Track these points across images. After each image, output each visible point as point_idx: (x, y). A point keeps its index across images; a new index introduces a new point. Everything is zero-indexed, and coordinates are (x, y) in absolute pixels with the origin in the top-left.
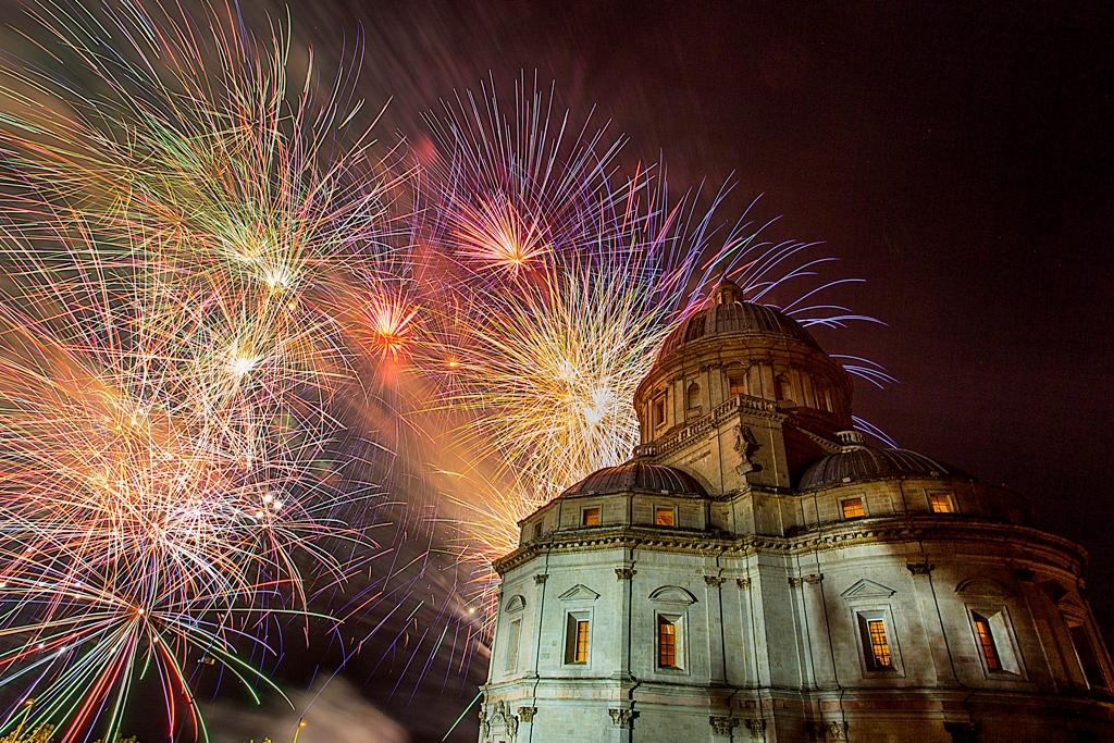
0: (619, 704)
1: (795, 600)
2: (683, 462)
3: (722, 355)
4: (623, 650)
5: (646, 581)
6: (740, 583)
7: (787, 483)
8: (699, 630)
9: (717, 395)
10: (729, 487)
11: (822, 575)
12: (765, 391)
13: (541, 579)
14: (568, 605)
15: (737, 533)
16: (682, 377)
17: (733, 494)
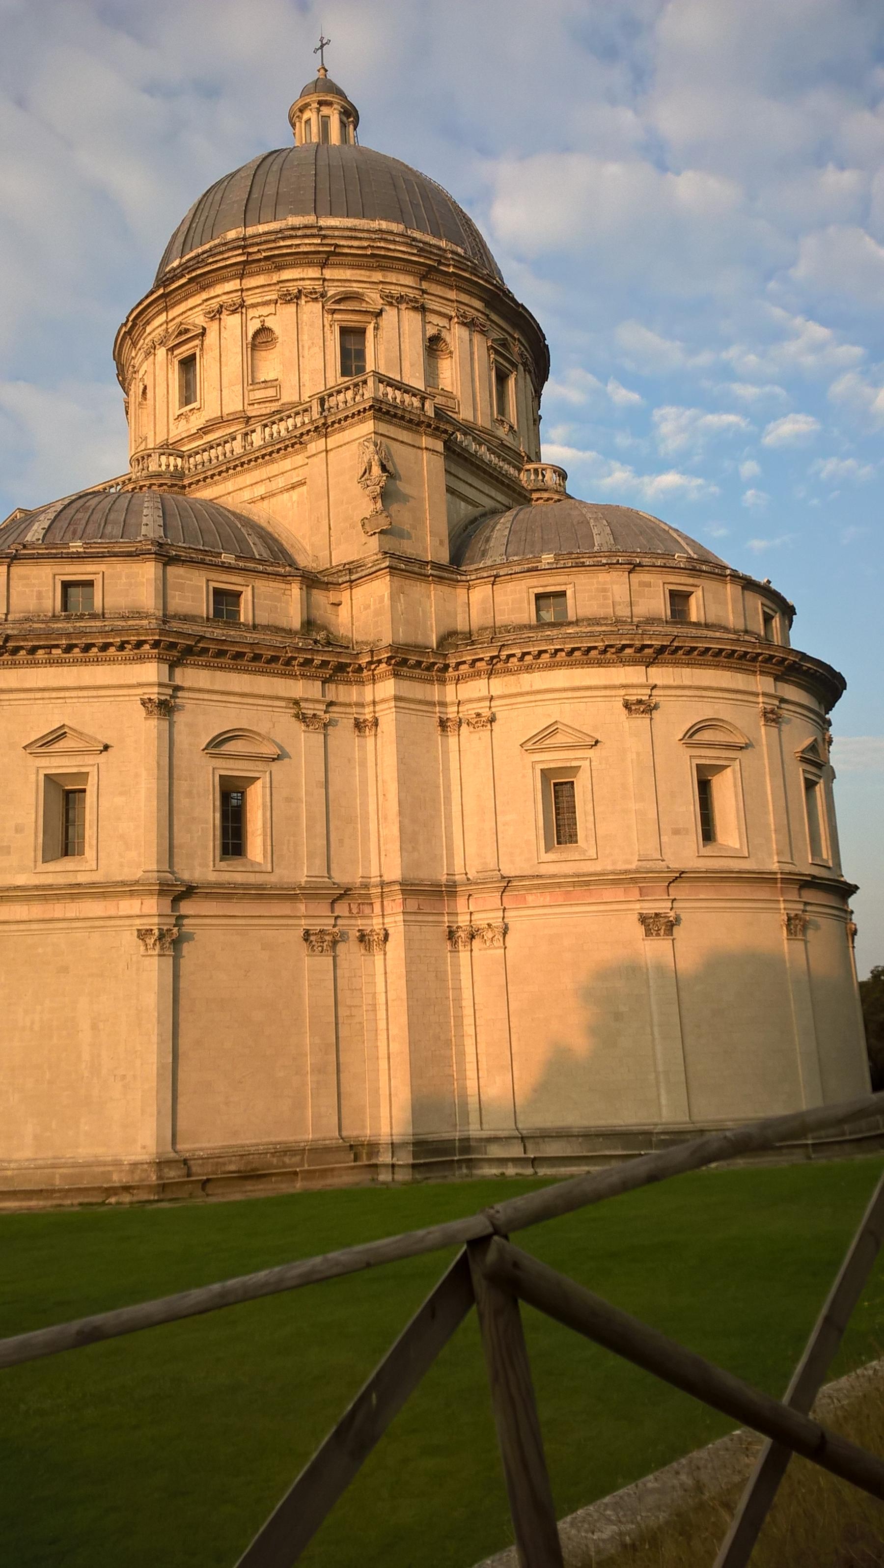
0: (156, 920)
1: (446, 753)
2: (247, 495)
3: (328, 273)
4: (160, 836)
5: (200, 722)
6: (359, 725)
7: (444, 557)
8: (288, 800)
9: (313, 360)
10: (341, 555)
11: (494, 714)
12: (406, 365)
14: (43, 762)
15: (357, 637)
16: (239, 307)
17: (350, 568)
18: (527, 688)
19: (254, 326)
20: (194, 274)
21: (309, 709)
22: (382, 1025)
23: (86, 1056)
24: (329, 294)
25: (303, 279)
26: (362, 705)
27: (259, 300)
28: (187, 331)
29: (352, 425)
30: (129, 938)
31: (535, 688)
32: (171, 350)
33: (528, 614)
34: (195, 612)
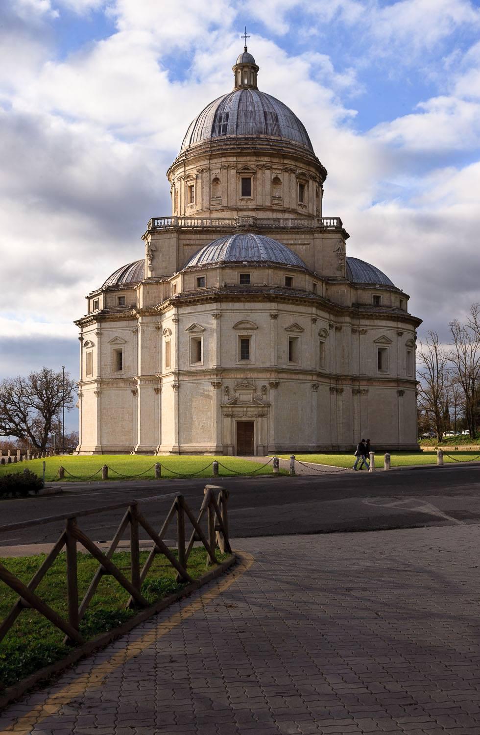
2: (285, 242)
6: (337, 328)
13: (275, 317)
14: (289, 333)
18: (376, 325)
19: (274, 176)
20: (256, 151)
21: (332, 323)
22: (341, 415)
23: (300, 417)
24: (299, 171)
25: (291, 165)
26: (338, 323)
27: (276, 167)
28: (248, 169)
29: (333, 233)
30: (309, 386)
31: (378, 325)
32: (240, 173)
33: (372, 301)
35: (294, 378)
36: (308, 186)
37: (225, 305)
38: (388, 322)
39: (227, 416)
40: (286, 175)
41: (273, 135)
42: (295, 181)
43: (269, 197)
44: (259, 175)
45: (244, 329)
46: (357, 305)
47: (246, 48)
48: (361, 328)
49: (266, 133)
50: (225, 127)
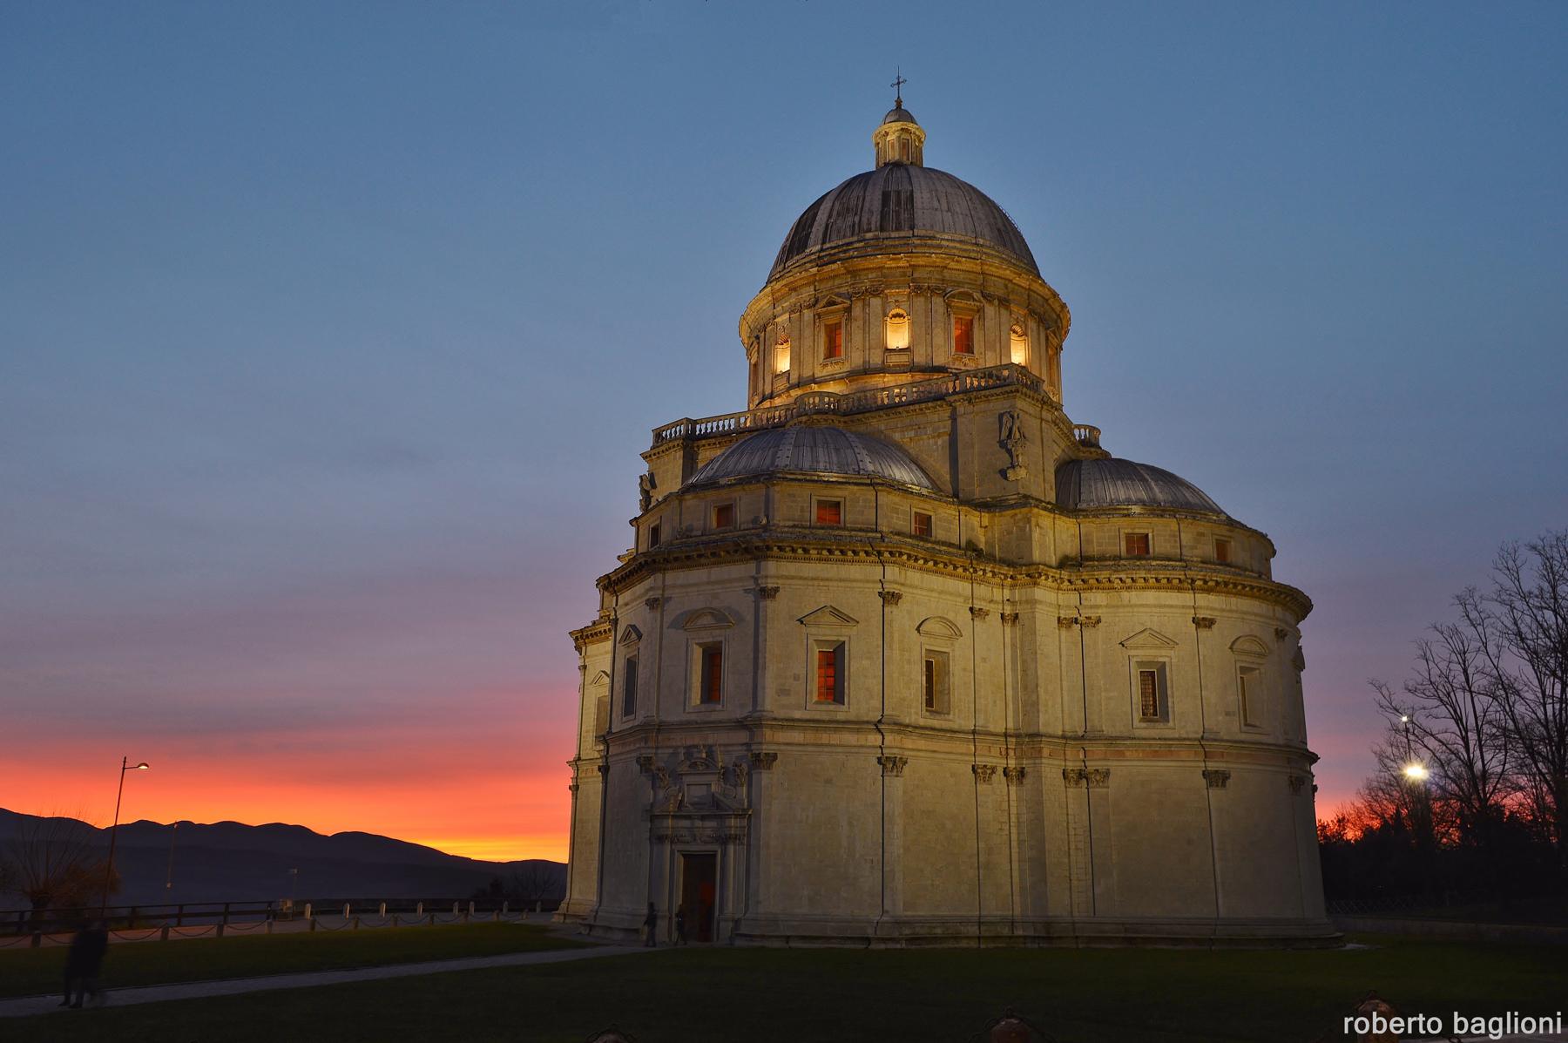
7: (1052, 497)
14: (813, 630)
28: (834, 303)
34: (907, 530)
35: (825, 741)
36: (982, 318)
37: (672, 577)
38: (1163, 594)
39: (661, 839)
40: (920, 302)
41: (898, 229)
42: (941, 310)
43: (879, 352)
44: (857, 310)
45: (705, 628)
46: (1075, 563)
47: (899, 103)
48: (1085, 613)
49: (882, 229)
50: (808, 236)
